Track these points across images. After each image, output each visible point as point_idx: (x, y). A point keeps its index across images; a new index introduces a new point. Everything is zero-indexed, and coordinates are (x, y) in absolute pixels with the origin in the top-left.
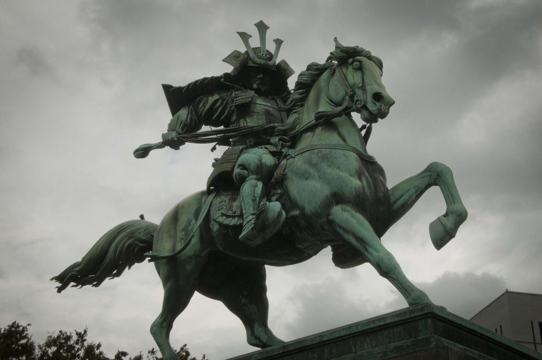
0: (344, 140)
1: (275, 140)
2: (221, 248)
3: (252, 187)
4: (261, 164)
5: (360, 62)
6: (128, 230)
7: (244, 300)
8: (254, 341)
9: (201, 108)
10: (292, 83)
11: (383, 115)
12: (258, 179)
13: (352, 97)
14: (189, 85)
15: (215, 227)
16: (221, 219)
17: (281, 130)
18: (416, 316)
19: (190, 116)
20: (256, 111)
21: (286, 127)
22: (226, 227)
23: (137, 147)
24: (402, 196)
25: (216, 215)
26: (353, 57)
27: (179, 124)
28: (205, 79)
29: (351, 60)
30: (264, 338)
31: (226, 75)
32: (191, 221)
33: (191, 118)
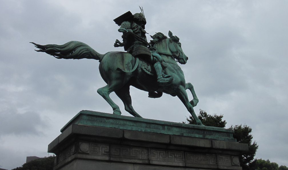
6: (86, 47)
8: (128, 110)
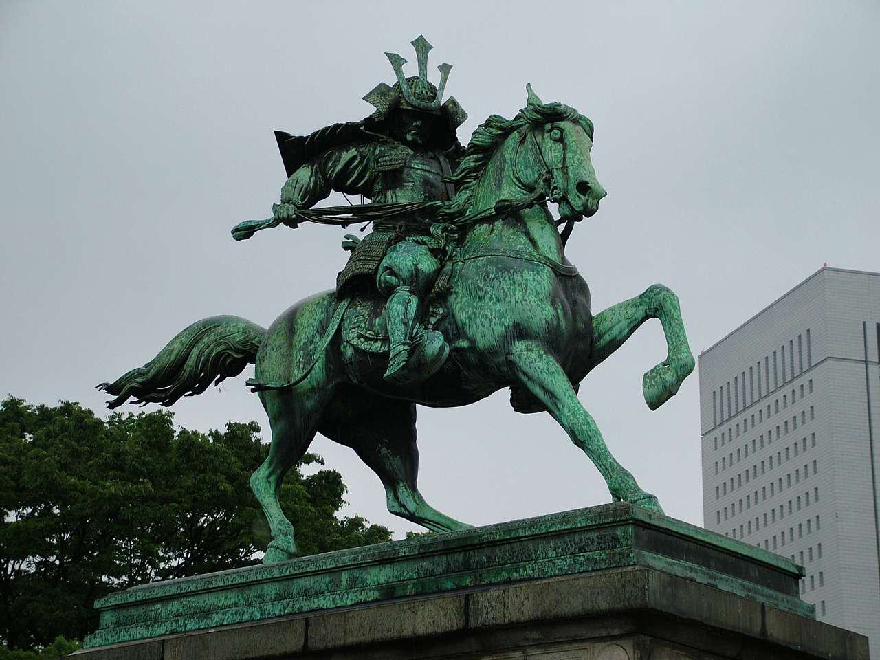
1: (436, 229)
2: (355, 381)
3: (402, 305)
4: (416, 269)
5: (562, 130)
7: (384, 451)
8: (397, 509)
9: (331, 167)
10: (464, 135)
11: (589, 212)
12: (412, 292)
13: (548, 181)
14: (314, 135)
15: (349, 352)
16: (355, 342)
17: (446, 214)
19: (313, 178)
21: (452, 211)
22: (365, 352)
23: (237, 224)
24: (610, 329)
25: (351, 336)
26: (553, 122)
28: (337, 126)
29: (548, 126)
30: (412, 507)
32: (313, 336)
33: (315, 183)
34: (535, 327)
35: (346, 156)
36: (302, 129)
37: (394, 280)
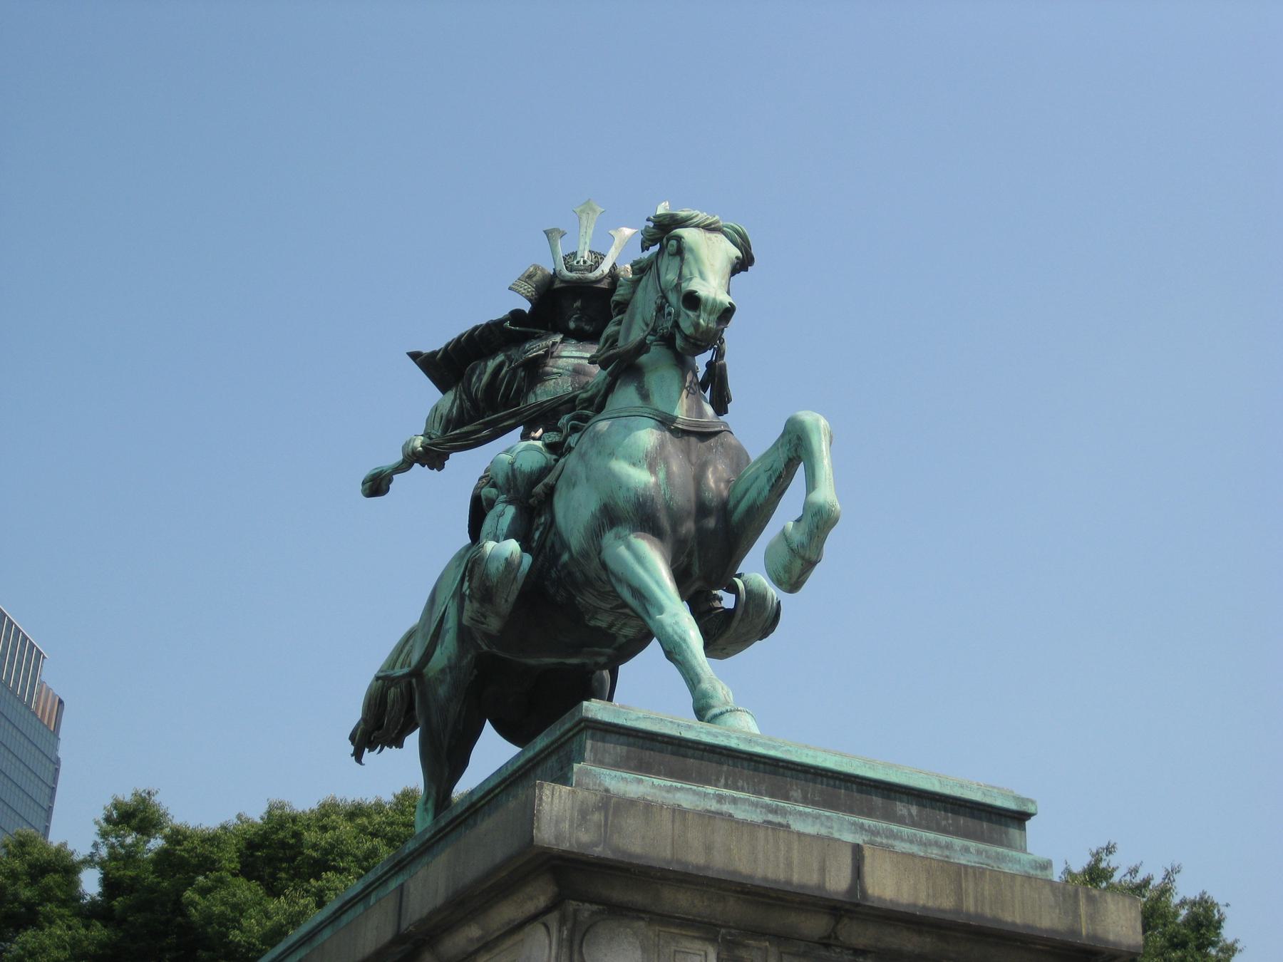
0: (645, 396)
4: (513, 470)
5: (679, 239)
12: (509, 502)
17: (585, 400)
18: (570, 730)
20: (555, 370)
24: (747, 491)
27: (438, 420)
28: (476, 328)
31: (516, 315)
33: (461, 407)
34: (621, 503)
35: (491, 365)
36: (435, 341)
37: (494, 491)
